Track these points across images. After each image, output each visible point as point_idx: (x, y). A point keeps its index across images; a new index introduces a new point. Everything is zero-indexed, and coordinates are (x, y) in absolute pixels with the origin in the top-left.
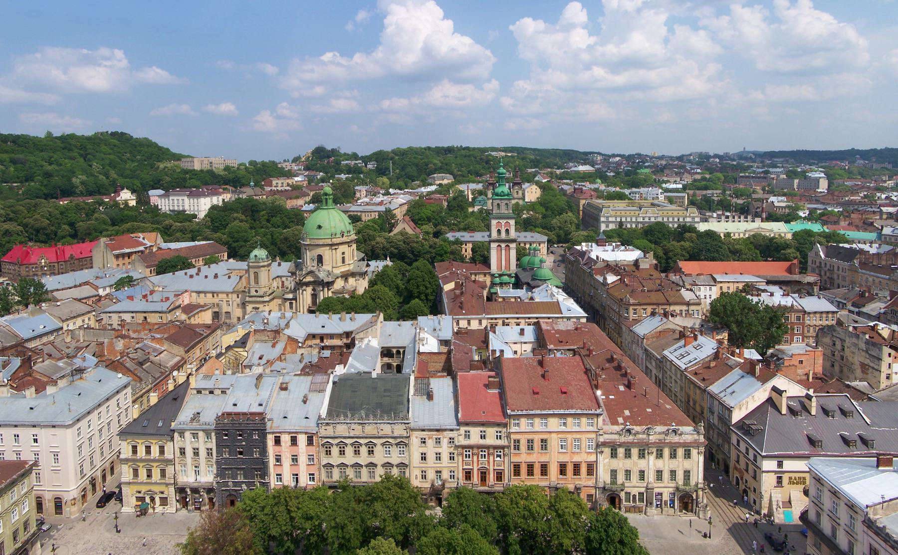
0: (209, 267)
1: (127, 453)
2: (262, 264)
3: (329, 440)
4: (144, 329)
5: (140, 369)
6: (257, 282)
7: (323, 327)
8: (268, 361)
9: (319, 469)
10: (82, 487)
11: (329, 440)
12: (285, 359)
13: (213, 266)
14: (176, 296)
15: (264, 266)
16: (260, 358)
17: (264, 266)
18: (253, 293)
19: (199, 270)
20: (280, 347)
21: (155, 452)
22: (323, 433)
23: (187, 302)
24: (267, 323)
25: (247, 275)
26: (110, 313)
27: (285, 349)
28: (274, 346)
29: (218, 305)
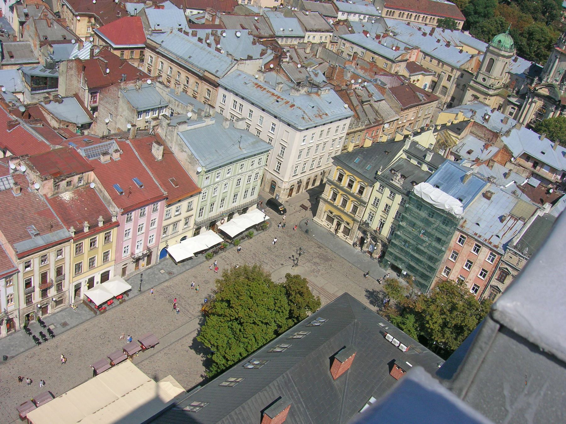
0: (443, 31)
1: (334, 177)
2: (503, 53)
3: (509, 268)
4: (371, 70)
5: (360, 106)
6: (489, 69)
7: (543, 153)
8: (477, 160)
9: (486, 287)
10: (292, 183)
11: (509, 268)
12: (492, 166)
13: (448, 31)
14: (406, 49)
15: (503, 56)
16: (469, 152)
17: (503, 56)
18: (480, 79)
19: (433, 31)
20: (493, 150)
21: (356, 188)
22: (506, 258)
23: (413, 59)
24: (487, 120)
25: (481, 58)
26: (345, 40)
27: (496, 155)
28: (486, 147)
29: (439, 76)
